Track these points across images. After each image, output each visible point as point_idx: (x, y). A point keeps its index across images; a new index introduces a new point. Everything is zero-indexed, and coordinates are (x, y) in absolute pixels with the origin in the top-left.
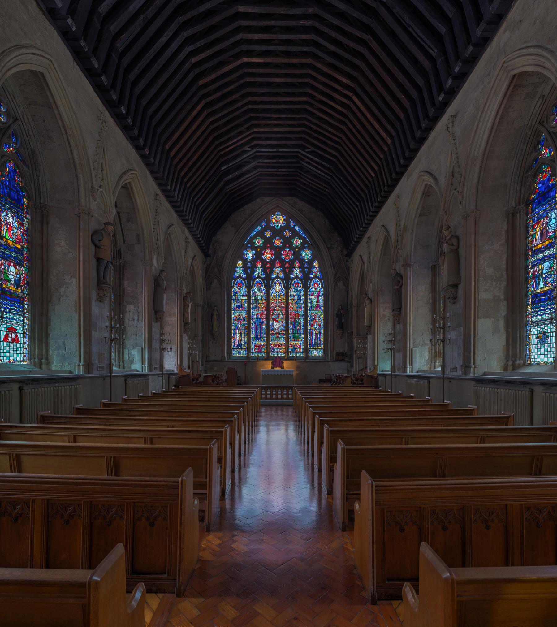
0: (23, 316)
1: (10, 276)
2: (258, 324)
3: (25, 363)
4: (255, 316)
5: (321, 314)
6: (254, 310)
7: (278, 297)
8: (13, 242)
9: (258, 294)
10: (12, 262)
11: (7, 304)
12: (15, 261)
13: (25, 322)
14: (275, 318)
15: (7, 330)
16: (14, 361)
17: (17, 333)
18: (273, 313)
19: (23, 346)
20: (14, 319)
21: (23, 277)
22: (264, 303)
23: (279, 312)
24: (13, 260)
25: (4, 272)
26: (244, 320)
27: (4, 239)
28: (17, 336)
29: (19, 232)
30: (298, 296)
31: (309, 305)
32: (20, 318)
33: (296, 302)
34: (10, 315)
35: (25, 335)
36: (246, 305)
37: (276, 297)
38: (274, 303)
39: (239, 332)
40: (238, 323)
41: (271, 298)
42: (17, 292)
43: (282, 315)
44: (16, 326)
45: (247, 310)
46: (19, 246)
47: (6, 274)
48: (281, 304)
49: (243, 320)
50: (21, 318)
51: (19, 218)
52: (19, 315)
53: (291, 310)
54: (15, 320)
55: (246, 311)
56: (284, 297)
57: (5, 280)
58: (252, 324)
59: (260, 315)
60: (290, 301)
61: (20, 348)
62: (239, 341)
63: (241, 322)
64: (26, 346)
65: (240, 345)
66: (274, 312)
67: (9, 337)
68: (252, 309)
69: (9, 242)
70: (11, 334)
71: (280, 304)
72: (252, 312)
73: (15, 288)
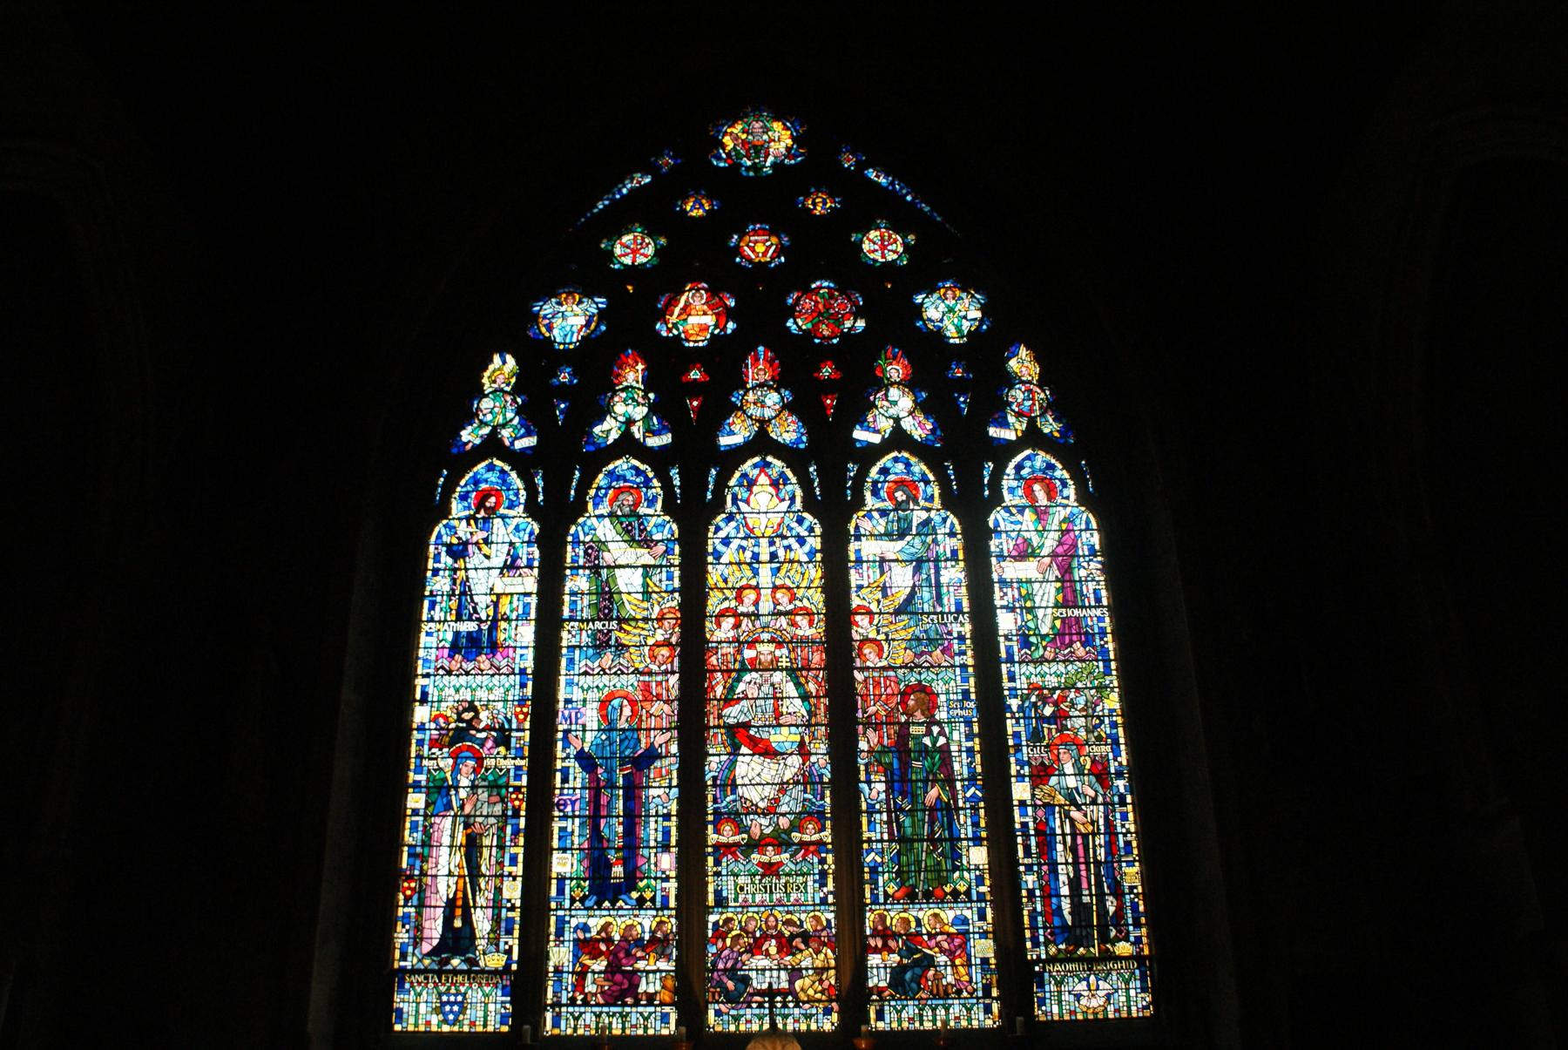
2: (610, 771)
4: (591, 717)
5: (1101, 688)
6: (580, 666)
7: (765, 571)
9: (619, 551)
14: (747, 726)
18: (731, 689)
22: (661, 619)
23: (778, 677)
26: (503, 738)
30: (919, 563)
31: (1006, 622)
33: (906, 608)
36: (526, 634)
37: (756, 573)
38: (736, 615)
39: (460, 838)
40: (456, 769)
41: (714, 576)
43: (805, 697)
45: (529, 664)
48: (794, 624)
49: (497, 744)
53: (872, 659)
55: (523, 672)
56: (815, 573)
58: (565, 771)
59: (633, 703)
60: (855, 602)
62: (450, 905)
63: (480, 760)
65: (458, 940)
66: (738, 680)
68: (571, 661)
71: (783, 621)
72: (570, 684)
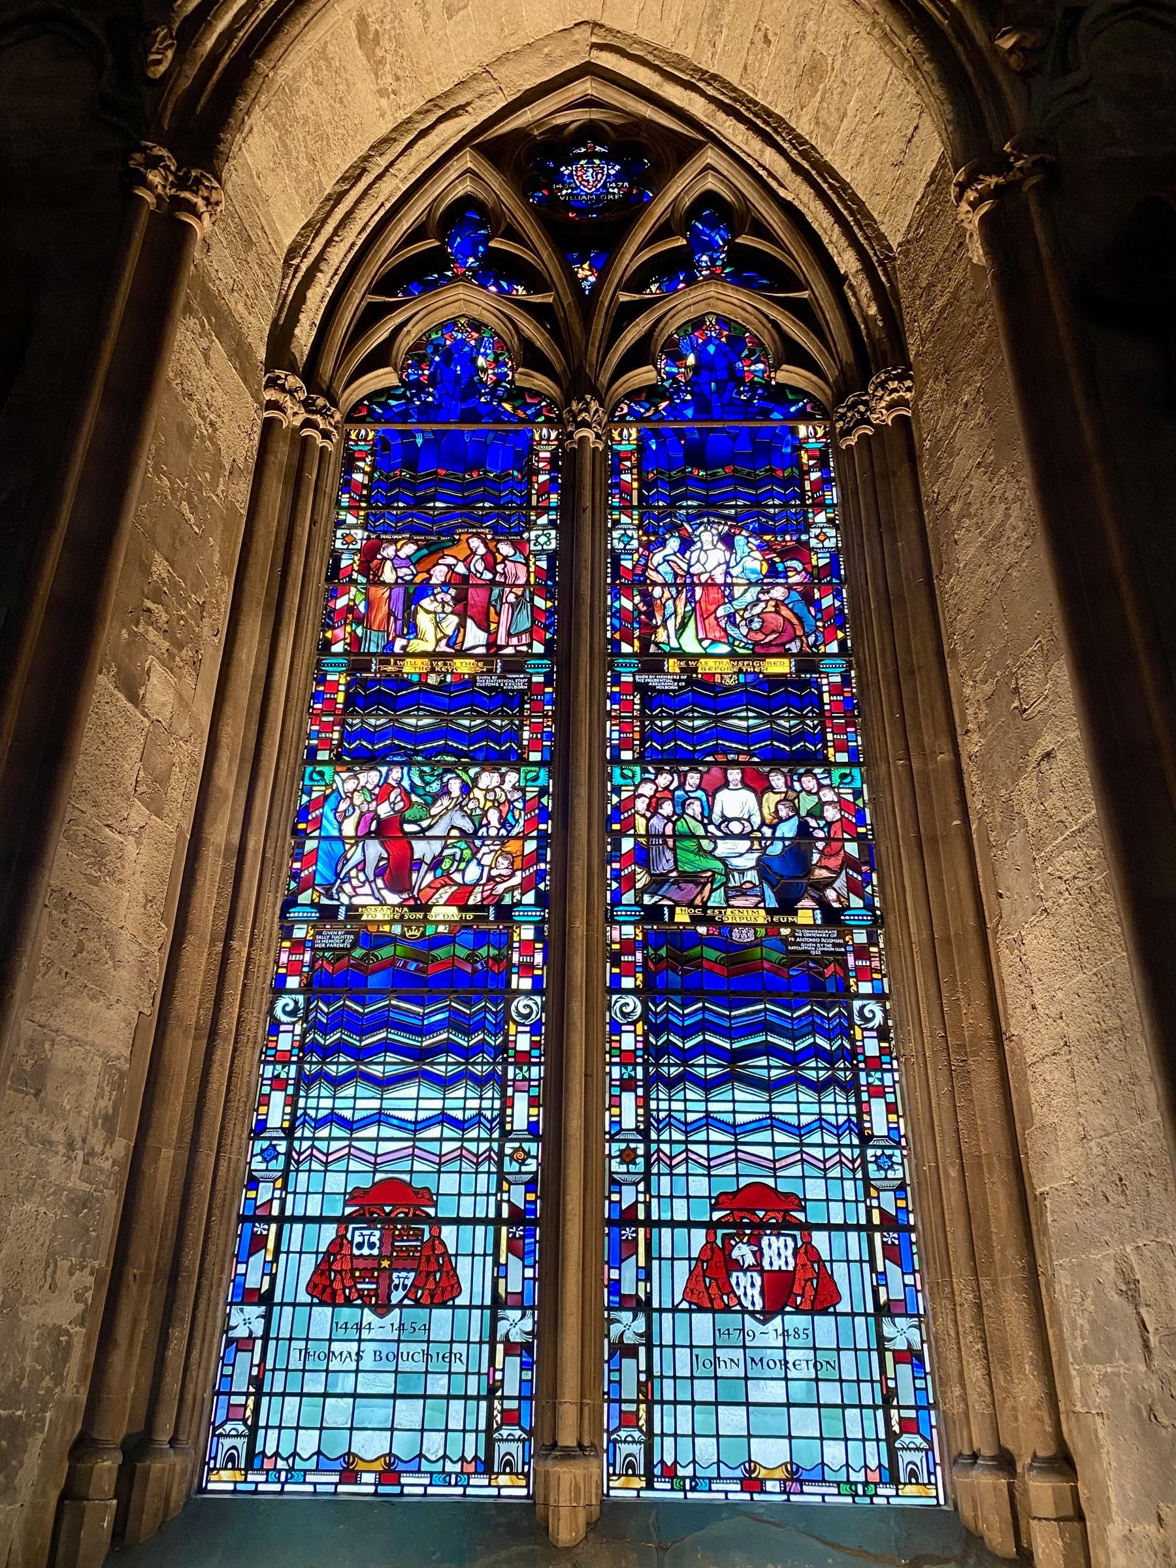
0: (850, 1087)
1: (724, 848)
3: (911, 1496)
8: (733, 656)
10: (735, 764)
11: (703, 1026)
12: (752, 754)
13: (880, 1129)
15: (717, 1215)
16: (794, 1476)
17: (808, 1228)
19: (881, 1339)
20: (772, 1122)
21: (829, 824)
24: (739, 752)
25: (676, 836)
27: (673, 665)
28: (806, 1253)
29: (778, 593)
32: (828, 1109)
34: (739, 1095)
35: (892, 1237)
42: (785, 931)
44: (796, 1171)
46: (779, 666)
47: (690, 844)
50: (837, 1107)
51: (772, 531)
52: (818, 1087)
54: (786, 1127)
57: (693, 878)
61: (847, 1358)
64: (915, 1336)
67: (737, 1266)
69: (707, 666)
70: (755, 1240)
73: (770, 912)
